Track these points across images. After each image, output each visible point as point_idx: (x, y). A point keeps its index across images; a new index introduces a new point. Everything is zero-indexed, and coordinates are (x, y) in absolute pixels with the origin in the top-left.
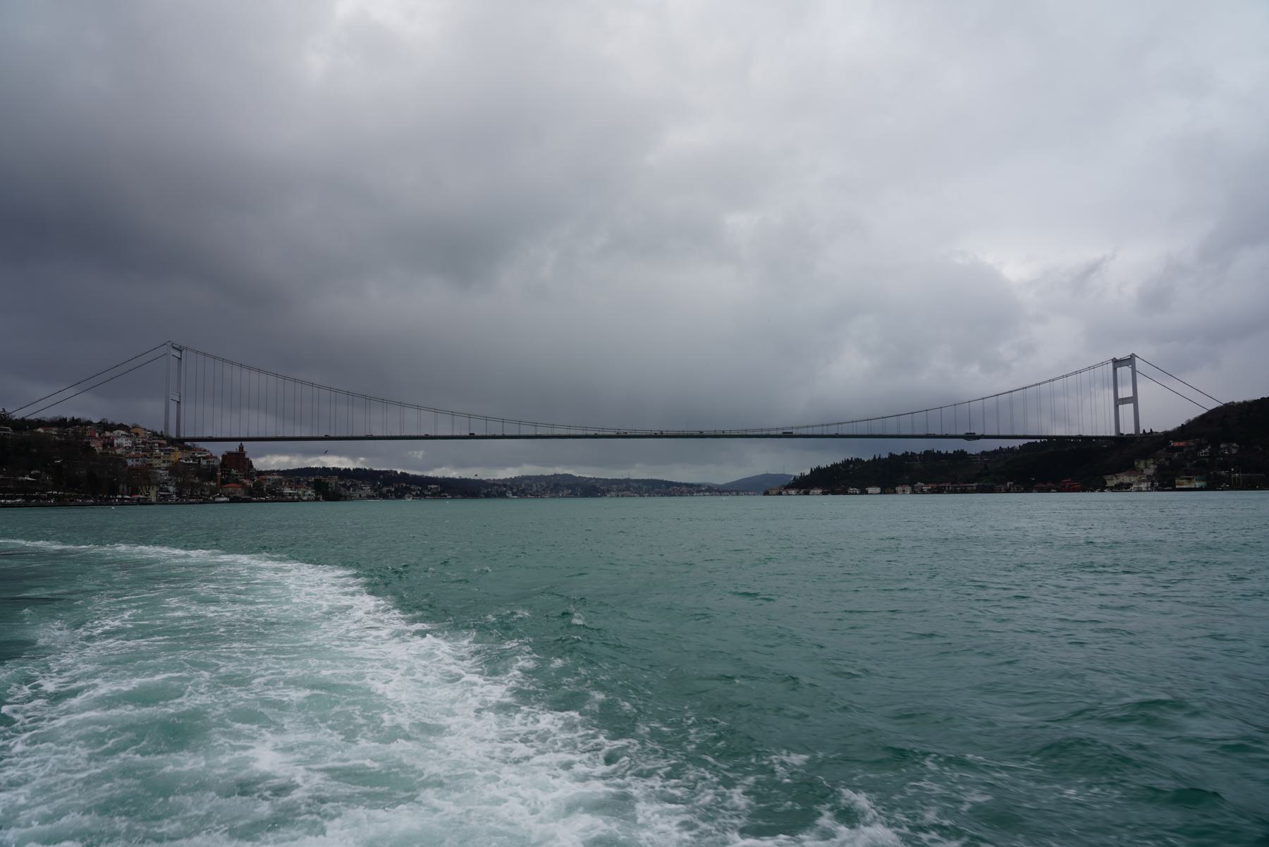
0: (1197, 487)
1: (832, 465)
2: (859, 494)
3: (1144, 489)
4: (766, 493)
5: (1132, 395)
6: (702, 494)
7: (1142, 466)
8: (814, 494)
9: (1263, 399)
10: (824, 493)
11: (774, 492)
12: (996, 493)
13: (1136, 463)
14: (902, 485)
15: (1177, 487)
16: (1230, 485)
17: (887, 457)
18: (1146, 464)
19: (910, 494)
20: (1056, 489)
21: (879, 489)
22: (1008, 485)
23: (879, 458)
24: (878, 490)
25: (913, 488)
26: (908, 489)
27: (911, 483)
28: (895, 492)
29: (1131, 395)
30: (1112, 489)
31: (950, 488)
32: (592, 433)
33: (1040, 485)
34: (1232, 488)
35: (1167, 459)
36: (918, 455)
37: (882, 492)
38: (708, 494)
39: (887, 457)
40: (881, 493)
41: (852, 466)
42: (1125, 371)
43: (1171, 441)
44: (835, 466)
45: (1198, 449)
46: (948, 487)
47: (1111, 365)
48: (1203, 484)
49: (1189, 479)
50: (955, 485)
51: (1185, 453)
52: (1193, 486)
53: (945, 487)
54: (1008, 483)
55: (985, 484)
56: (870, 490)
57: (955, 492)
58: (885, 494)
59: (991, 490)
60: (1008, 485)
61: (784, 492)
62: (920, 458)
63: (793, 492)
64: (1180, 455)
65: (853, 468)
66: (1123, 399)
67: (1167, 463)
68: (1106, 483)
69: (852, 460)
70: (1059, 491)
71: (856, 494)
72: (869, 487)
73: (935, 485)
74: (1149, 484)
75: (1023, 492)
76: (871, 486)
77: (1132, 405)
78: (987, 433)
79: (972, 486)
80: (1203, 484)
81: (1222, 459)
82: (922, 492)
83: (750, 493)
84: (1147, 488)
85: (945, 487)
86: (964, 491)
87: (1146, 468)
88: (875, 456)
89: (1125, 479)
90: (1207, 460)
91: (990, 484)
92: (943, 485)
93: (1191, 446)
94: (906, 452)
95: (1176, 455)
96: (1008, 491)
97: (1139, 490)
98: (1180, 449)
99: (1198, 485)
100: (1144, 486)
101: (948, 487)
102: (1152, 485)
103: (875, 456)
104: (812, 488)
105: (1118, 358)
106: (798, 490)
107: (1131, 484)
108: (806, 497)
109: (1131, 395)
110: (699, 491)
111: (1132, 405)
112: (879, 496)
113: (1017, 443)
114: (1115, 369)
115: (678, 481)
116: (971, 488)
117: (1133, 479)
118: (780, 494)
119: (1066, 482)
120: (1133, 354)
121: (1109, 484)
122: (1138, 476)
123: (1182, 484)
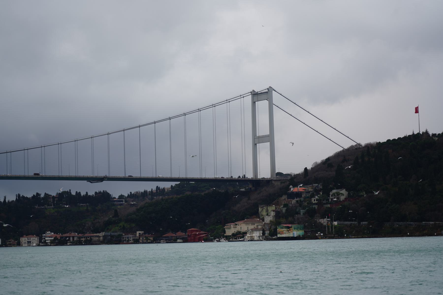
0: (295, 236)
3: (256, 238)
5: (269, 134)
7: (264, 213)
9: (389, 141)
12: (123, 243)
13: (260, 209)
14: (28, 234)
15: (279, 236)
16: (325, 234)
17: (15, 199)
18: (267, 211)
19: (39, 245)
20: (182, 239)
22: (138, 235)
26: (35, 240)
27: (39, 234)
28: (19, 244)
29: (268, 133)
30: (228, 238)
31: (75, 239)
33: (170, 234)
34: (325, 237)
35: (285, 206)
39: (15, 199)
42: (262, 105)
43: (291, 186)
45: (313, 196)
46: (73, 237)
47: (249, 99)
48: (300, 233)
49: (288, 228)
50: (80, 235)
51: (302, 199)
52: (291, 235)
53: (69, 237)
54: (138, 233)
55: (113, 234)
57: (79, 243)
58: (6, 246)
60: (138, 235)
62: (54, 201)
64: (297, 201)
66: (259, 137)
67: (284, 210)
68: (225, 232)
70: (185, 241)
73: (59, 236)
74: (261, 232)
75: (152, 242)
77: (268, 144)
78: (112, 175)
79: (99, 237)
80: (300, 233)
81: (329, 206)
82: (46, 244)
84: (259, 237)
85: (69, 237)
87: (267, 215)
89: (242, 227)
90: (316, 207)
92: (68, 235)
93: (309, 192)
94: (37, 194)
95: (294, 201)
96: (136, 242)
97: (252, 240)
98: (298, 195)
99: (296, 233)
100: (256, 234)
101: (73, 237)
102: (264, 234)
105: (257, 90)
107: (245, 233)
109: (268, 133)
111: (268, 144)
113: (150, 186)
114: (254, 103)
116: (97, 238)
117: (251, 227)
119: (192, 231)
120: (270, 87)
121: (229, 232)
122: (256, 225)
123: (282, 233)
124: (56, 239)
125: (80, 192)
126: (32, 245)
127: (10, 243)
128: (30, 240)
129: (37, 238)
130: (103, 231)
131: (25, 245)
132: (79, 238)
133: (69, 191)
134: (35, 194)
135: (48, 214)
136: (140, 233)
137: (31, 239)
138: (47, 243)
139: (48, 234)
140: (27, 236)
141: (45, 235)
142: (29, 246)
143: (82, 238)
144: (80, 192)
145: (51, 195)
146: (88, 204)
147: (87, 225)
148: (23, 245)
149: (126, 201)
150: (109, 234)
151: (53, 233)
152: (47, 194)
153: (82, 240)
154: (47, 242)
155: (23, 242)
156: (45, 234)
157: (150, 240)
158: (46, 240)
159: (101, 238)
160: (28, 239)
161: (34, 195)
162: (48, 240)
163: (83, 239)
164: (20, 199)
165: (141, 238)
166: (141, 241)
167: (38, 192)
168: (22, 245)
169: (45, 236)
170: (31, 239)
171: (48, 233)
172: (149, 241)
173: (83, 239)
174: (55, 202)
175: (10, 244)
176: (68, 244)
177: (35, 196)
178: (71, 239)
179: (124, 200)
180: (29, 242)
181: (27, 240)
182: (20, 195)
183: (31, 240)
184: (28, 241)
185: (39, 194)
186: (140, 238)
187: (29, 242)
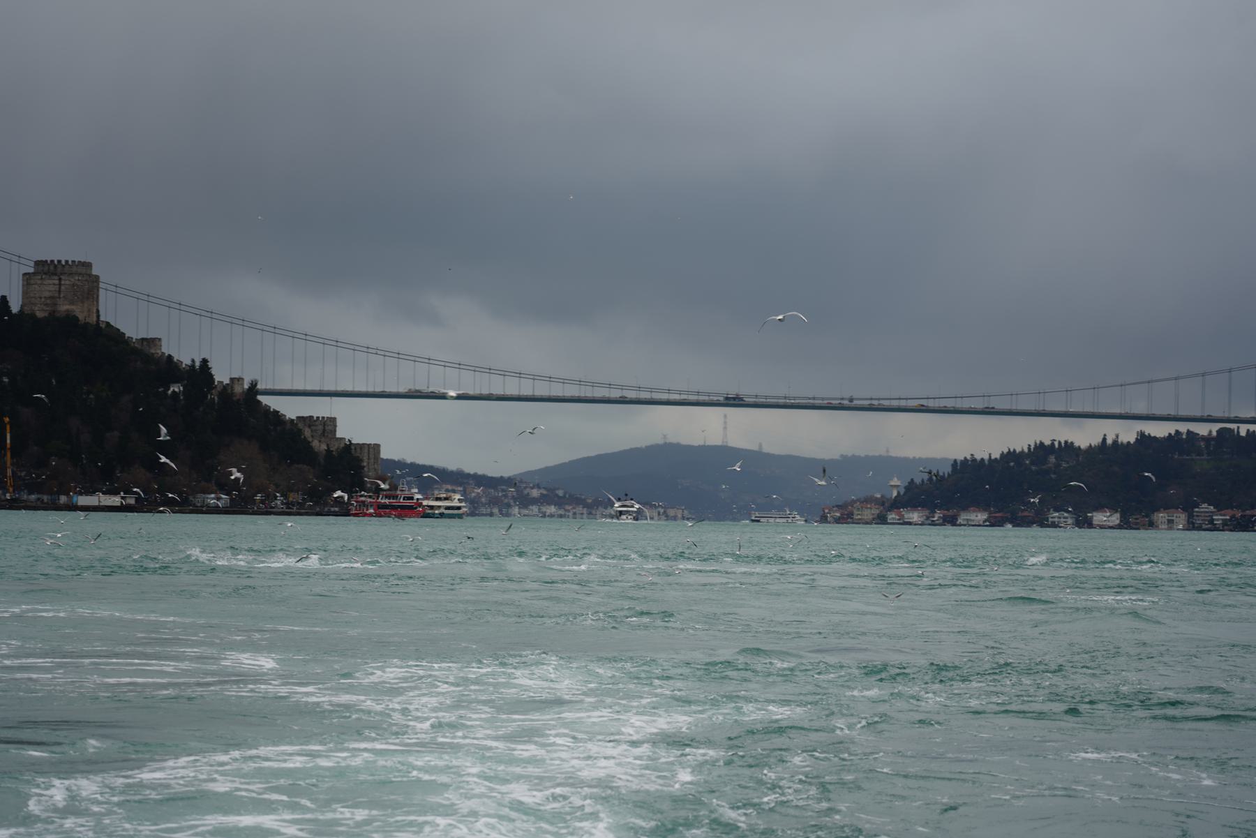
1: (1002, 454)
4: (846, 516)
6: (535, 509)
8: (969, 524)
10: (994, 523)
11: (868, 514)
14: (1167, 507)
21: (1117, 515)
23: (1115, 442)
24: (1115, 519)
25: (1190, 516)
26: (1181, 518)
28: (1151, 525)
32: (615, 394)
36: (1203, 438)
37: (1125, 525)
38: (552, 509)
39: (1132, 440)
40: (1119, 527)
41: (1052, 459)
44: (1010, 456)
56: (1099, 517)
61: (892, 516)
63: (915, 516)
65: (1058, 466)
69: (1053, 444)
76: (1099, 508)
82: (1214, 528)
83: (671, 512)
88: (1104, 440)
103: (1104, 440)
104: (965, 508)
106: (927, 512)
108: (949, 529)
110: (525, 502)
112: (1117, 532)
118: (881, 520)
124: (1233, 517)
126: (1175, 527)
127: (1138, 521)
128: (1172, 518)
129: (1184, 515)
131: (1163, 527)
133: (1236, 430)
134: (1173, 433)
135: (1199, 470)
137: (1175, 515)
138: (1216, 524)
139: (1203, 508)
140: (1166, 511)
141: (1197, 510)
142: (1170, 528)
145: (1198, 434)
148: (1160, 527)
151: (1212, 507)
152: (1192, 432)
154: (1215, 522)
155: (1160, 521)
156: (1198, 508)
158: (1213, 520)
160: (1169, 516)
161: (1170, 434)
162: (1218, 520)
164: (1143, 439)
167: (1177, 429)
168: (1157, 527)
169: (1197, 512)
170: (1173, 516)
171: (1203, 506)
174: (1212, 449)
175: (1137, 524)
177: (1184, 437)
180: (1171, 522)
181: (1167, 518)
182: (1144, 432)
183: (1174, 518)
185: (1180, 432)
187: (1171, 522)
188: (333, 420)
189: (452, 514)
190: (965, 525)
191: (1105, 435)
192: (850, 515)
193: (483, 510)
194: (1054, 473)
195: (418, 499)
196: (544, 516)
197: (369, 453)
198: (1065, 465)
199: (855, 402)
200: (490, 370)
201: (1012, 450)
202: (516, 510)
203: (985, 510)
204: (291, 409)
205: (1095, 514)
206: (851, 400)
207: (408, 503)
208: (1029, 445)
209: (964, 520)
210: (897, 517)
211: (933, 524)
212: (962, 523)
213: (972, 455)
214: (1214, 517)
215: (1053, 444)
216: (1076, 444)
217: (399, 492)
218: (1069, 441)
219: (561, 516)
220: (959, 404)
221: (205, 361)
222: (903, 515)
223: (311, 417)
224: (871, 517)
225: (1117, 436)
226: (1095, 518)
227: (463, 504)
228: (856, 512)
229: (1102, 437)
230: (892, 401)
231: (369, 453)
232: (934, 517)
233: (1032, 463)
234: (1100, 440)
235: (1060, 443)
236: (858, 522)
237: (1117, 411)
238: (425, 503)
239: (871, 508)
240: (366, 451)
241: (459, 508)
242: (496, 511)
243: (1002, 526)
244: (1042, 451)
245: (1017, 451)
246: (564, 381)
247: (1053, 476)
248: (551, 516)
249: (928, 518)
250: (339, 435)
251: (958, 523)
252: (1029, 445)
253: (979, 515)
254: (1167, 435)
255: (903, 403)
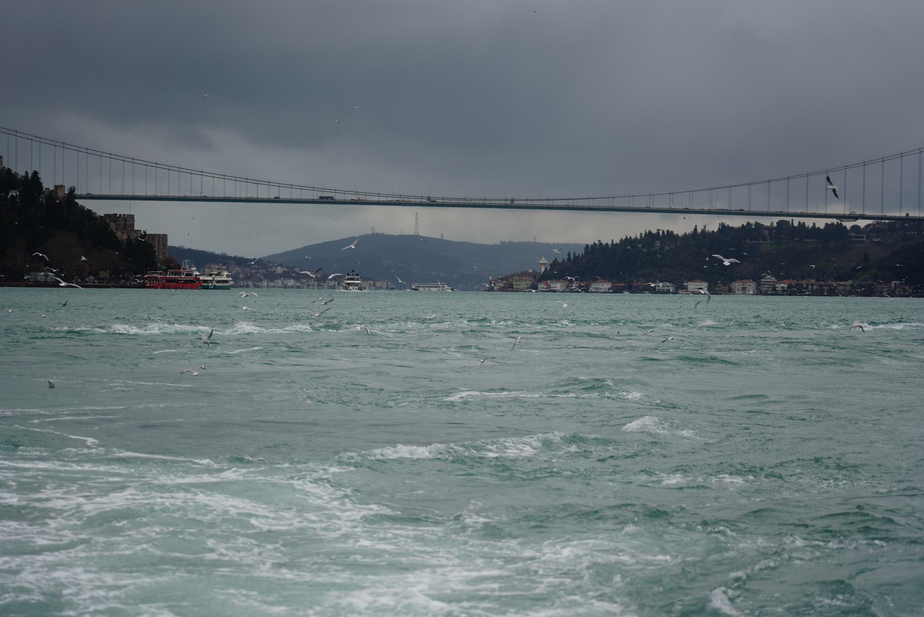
1: (621, 240)
2: (673, 293)
4: (509, 287)
6: (279, 282)
10: (616, 290)
11: (524, 284)
12: (875, 296)
22: (893, 285)
23: (703, 231)
25: (759, 285)
26: (751, 286)
27: (756, 278)
28: (730, 291)
31: (815, 287)
36: (767, 228)
38: (291, 282)
39: (716, 230)
41: (658, 243)
44: (627, 242)
46: (812, 285)
54: (893, 283)
56: (692, 286)
57: (819, 293)
59: (869, 292)
61: (541, 286)
62: (770, 234)
63: (558, 286)
65: (662, 248)
69: (658, 233)
71: (668, 292)
72: (690, 280)
73: (794, 282)
82: (775, 293)
83: (378, 284)
86: (832, 293)
88: (696, 229)
91: (870, 282)
96: (892, 294)
101: (812, 285)
103: (696, 229)
104: (595, 280)
110: (272, 277)
115: (218, 251)
118: (534, 287)
124: (790, 286)
125: (804, 223)
130: (850, 279)
132: (821, 286)
133: (791, 222)
134: (745, 224)
136: (895, 284)
141: (763, 280)
142: (744, 294)
143: (824, 286)
144: (804, 223)
146: (816, 240)
147: (828, 271)
149: (867, 238)
150: (858, 282)
152: (759, 224)
153: (824, 290)
157: (908, 292)
158: (776, 287)
159: (848, 288)
161: (743, 225)
163: (826, 288)
164: (724, 228)
165: (897, 290)
166: (897, 293)
168: (734, 293)
172: (907, 293)
173: (826, 288)
176: (807, 293)
177: (753, 227)
178: (810, 287)
179: (865, 236)
180: (744, 289)
184: (743, 288)
186: (895, 290)
187: (744, 289)
188: (132, 217)
189: (222, 286)
190: (595, 292)
191: (696, 226)
192: (511, 286)
193: (241, 283)
194: (660, 254)
195: (196, 275)
196: (285, 287)
197: (159, 242)
198: (667, 248)
199: (515, 202)
200: (247, 180)
201: (628, 237)
202: (265, 283)
203: (609, 281)
204: (100, 209)
205: (689, 283)
206: (512, 201)
207: (189, 278)
208: (641, 234)
209: (594, 288)
210: (545, 287)
211: (572, 291)
212: (593, 291)
213: (599, 241)
214: (776, 286)
215: (658, 233)
216: (675, 233)
217: (182, 270)
218: (670, 231)
219: (298, 287)
220: (592, 203)
221: (35, 173)
222: (550, 285)
223: (115, 215)
224: (526, 286)
225: (705, 227)
226: (689, 287)
227: (230, 279)
228: (515, 283)
229: (694, 227)
230: (543, 202)
231: (159, 242)
232: (572, 286)
233: (643, 247)
234: (693, 230)
235: (663, 232)
236: (517, 291)
237: (706, 208)
238: (202, 278)
239: (526, 280)
240: (157, 239)
241: (227, 282)
242: (251, 283)
243: (622, 293)
244: (650, 237)
245: (632, 238)
246: (301, 188)
247: (659, 256)
248: (292, 287)
249: (567, 287)
250: (136, 228)
251: (590, 290)
252: (641, 234)
253: (605, 285)
254: (741, 226)
255: (550, 203)
